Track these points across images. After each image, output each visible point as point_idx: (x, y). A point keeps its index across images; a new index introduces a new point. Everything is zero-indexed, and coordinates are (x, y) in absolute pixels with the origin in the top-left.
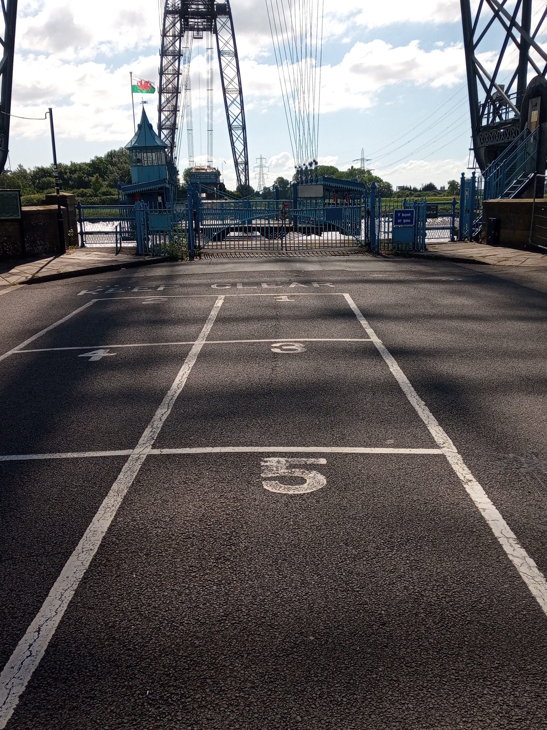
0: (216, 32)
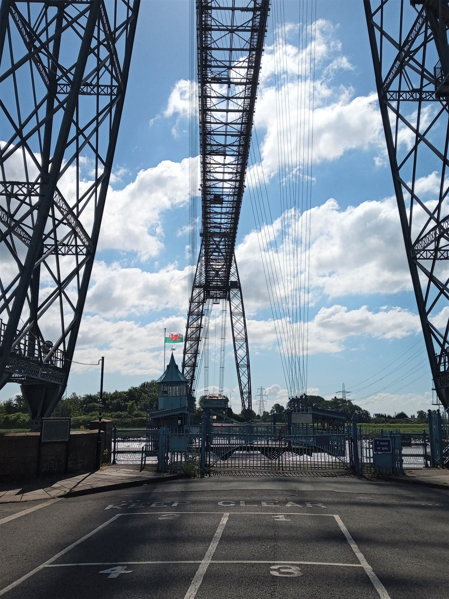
0: (229, 299)
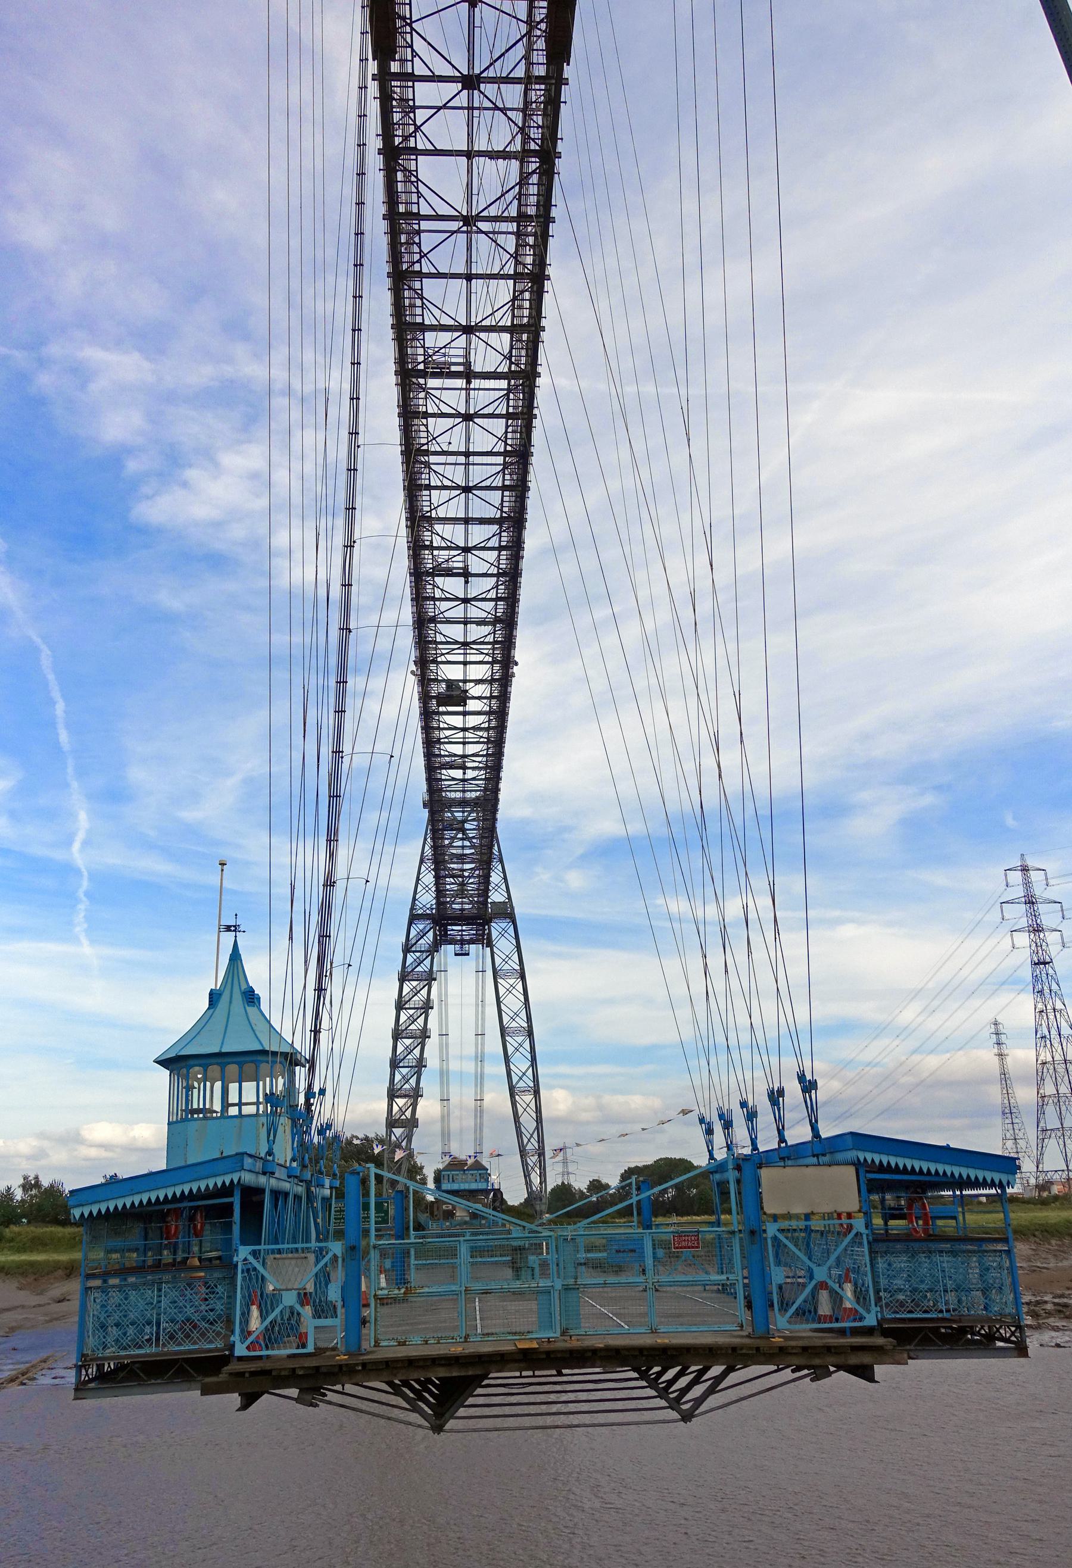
0: (490, 944)
